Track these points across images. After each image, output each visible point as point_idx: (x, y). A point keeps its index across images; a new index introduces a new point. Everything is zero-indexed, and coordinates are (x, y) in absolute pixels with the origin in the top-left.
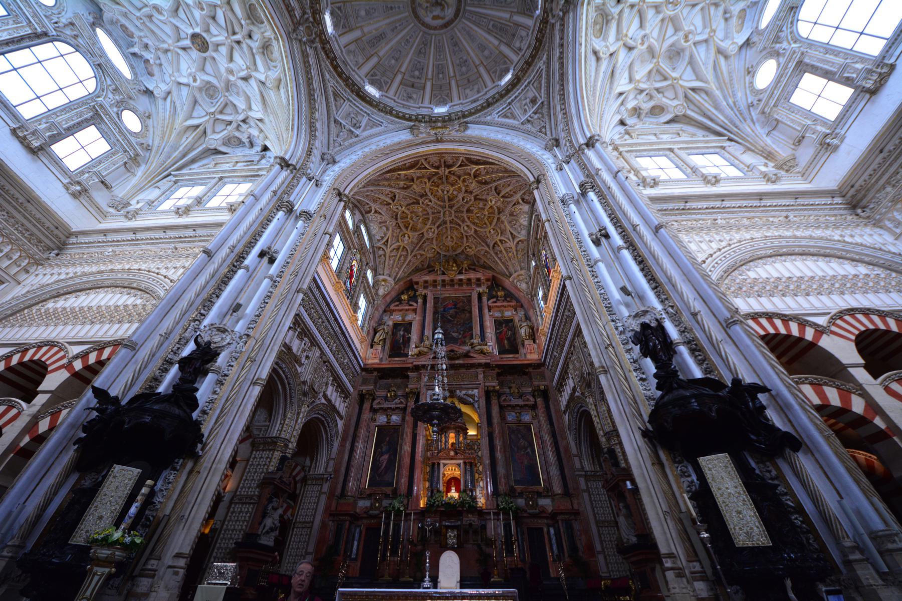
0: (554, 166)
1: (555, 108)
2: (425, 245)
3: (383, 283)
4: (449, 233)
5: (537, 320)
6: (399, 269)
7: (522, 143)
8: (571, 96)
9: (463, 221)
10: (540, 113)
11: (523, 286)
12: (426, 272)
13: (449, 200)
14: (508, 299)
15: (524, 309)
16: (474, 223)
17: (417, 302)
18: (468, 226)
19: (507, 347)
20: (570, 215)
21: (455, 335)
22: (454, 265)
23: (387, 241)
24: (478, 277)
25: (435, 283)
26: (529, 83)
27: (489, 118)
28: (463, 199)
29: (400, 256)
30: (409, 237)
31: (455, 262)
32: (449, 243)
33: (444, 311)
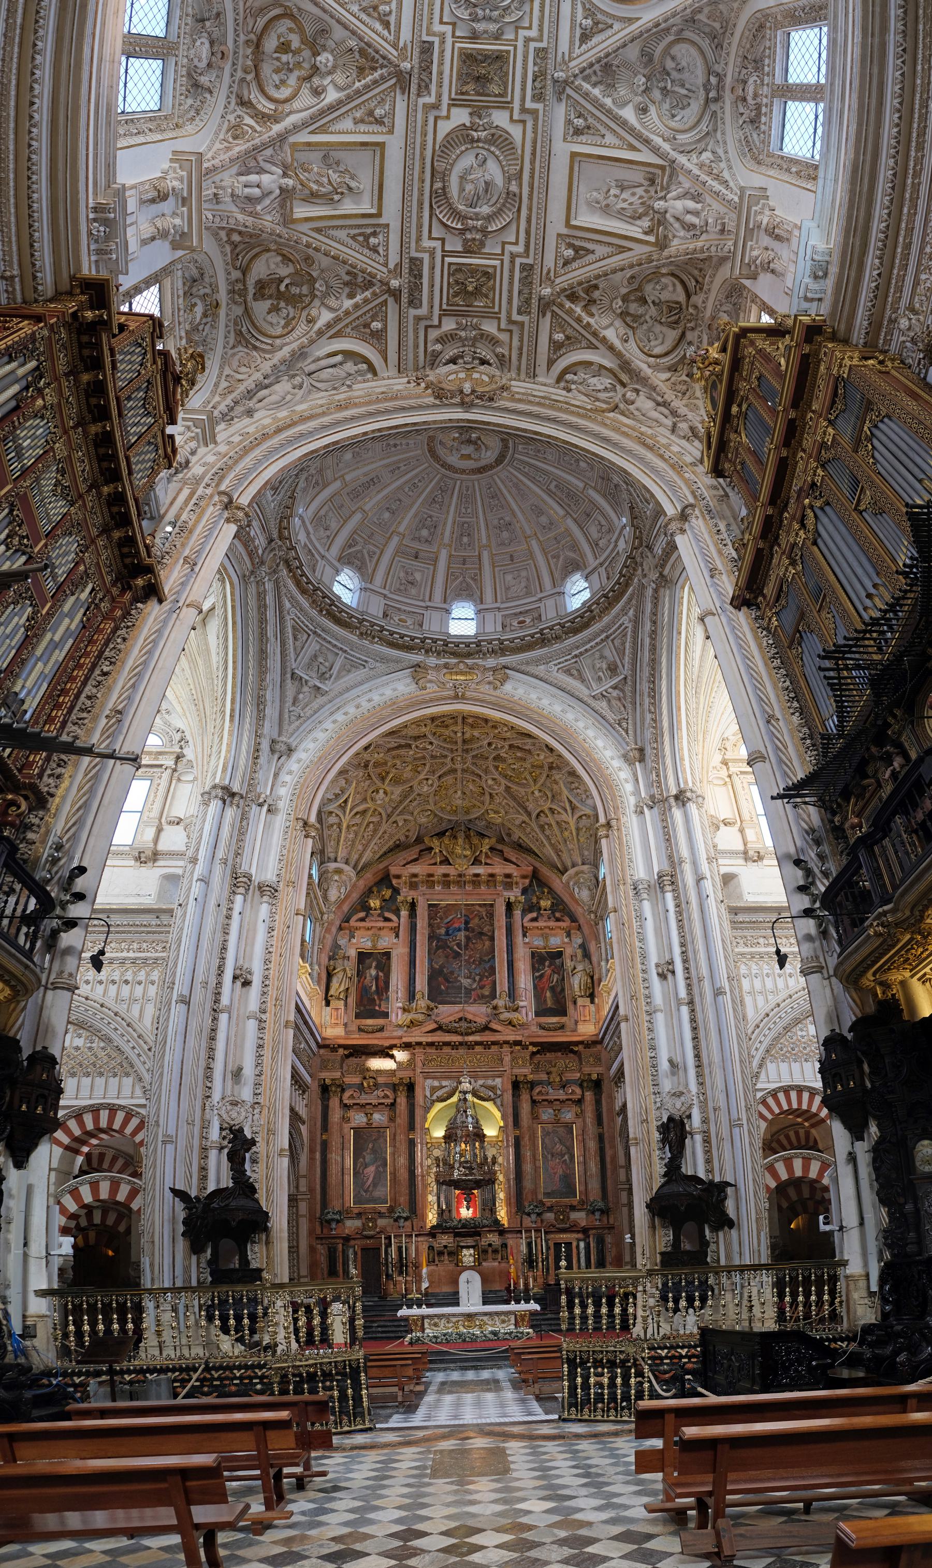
0: (632, 800)
1: (642, 695)
2: (415, 804)
3: (336, 877)
4: (459, 785)
5: (599, 964)
6: (365, 847)
7: (591, 733)
8: (664, 698)
9: (486, 771)
10: (622, 691)
11: (585, 895)
12: (413, 853)
13: (464, 741)
14: (558, 915)
15: (582, 933)
16: (505, 776)
17: (397, 912)
18: (494, 779)
19: (549, 1003)
20: (640, 917)
21: (466, 982)
22: (467, 847)
23: (346, 801)
24: (507, 871)
25: (430, 881)
26: (607, 637)
27: (542, 667)
28: (490, 744)
29: (368, 825)
30: (385, 793)
31: (468, 837)
32: (459, 802)
33: (447, 934)
